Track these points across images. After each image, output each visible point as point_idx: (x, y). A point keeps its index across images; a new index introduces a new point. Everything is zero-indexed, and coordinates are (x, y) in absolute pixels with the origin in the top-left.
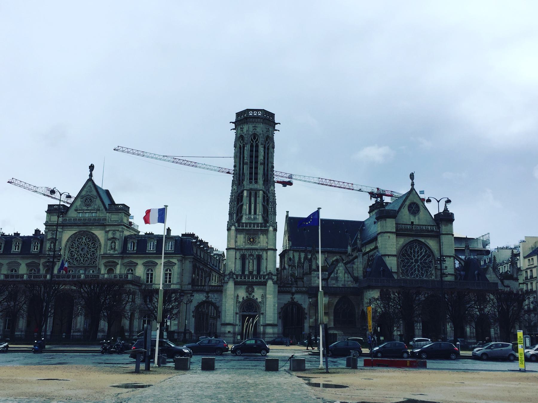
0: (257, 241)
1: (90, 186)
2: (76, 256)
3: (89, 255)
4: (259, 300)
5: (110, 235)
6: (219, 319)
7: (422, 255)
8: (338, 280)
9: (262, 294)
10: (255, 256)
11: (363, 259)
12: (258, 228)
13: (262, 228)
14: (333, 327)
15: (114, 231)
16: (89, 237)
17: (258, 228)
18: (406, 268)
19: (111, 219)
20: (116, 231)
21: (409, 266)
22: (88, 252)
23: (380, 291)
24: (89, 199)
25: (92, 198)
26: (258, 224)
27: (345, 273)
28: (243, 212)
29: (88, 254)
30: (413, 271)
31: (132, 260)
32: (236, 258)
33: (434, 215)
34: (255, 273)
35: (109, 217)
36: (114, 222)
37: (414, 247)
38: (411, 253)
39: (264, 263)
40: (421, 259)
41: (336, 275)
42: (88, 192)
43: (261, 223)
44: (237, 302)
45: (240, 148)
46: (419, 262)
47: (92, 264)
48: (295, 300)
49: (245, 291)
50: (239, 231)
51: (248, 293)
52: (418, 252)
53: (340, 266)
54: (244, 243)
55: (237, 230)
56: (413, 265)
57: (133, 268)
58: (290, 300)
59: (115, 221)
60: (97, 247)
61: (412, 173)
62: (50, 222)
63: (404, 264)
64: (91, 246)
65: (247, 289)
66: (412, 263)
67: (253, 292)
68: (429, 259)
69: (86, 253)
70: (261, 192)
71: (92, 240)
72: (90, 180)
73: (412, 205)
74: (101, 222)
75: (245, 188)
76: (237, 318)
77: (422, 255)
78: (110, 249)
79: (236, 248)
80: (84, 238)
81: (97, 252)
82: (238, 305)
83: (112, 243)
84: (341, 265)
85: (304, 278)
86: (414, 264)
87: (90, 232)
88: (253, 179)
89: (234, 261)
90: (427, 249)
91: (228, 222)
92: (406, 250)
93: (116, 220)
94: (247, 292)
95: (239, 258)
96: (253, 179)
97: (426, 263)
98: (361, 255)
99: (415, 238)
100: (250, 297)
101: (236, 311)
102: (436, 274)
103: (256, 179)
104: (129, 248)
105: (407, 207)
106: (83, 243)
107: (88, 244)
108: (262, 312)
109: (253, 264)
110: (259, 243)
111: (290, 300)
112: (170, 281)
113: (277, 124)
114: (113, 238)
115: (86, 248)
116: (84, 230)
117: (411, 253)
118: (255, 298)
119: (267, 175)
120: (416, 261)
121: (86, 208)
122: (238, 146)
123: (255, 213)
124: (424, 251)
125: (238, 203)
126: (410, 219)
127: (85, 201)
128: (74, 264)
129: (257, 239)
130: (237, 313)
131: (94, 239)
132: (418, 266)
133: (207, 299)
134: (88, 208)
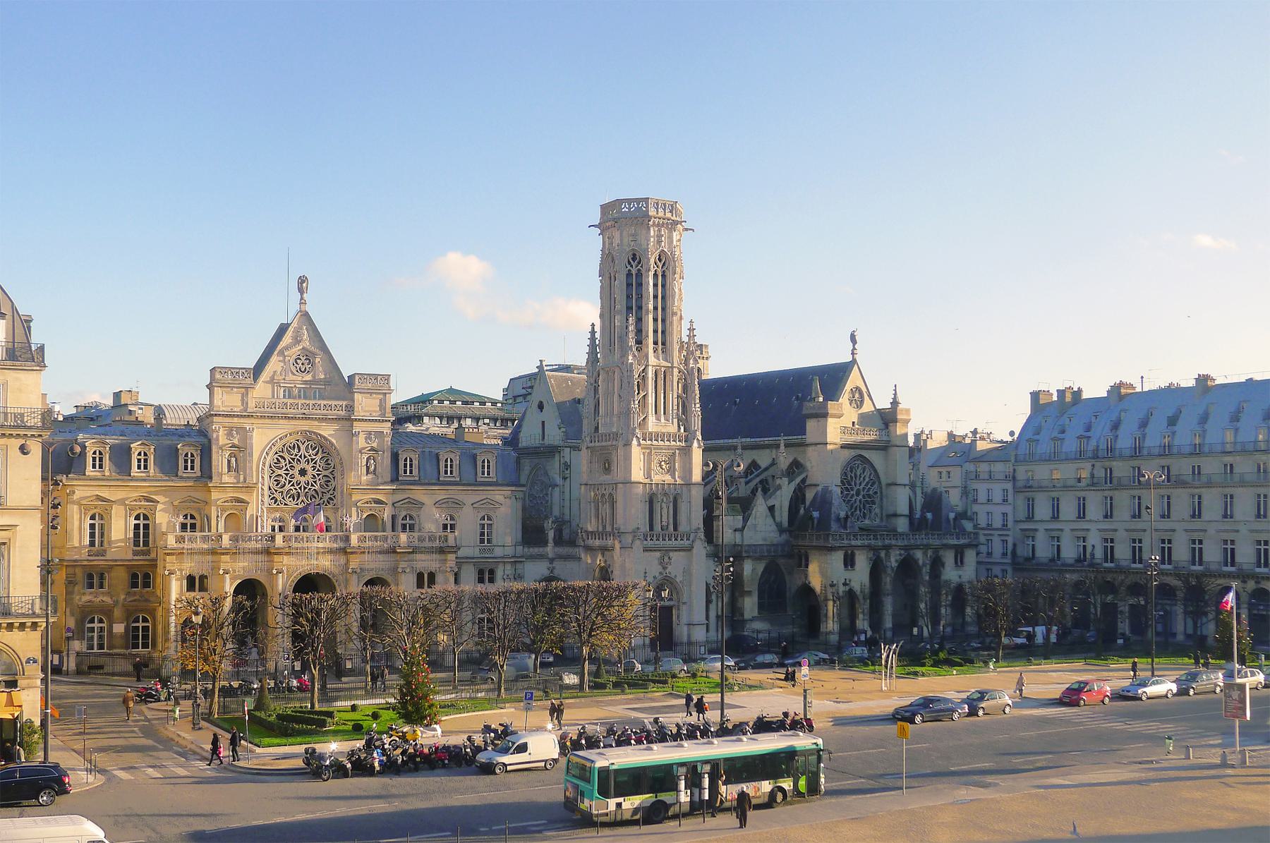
2: (287, 487)
10: (671, 496)
27: (766, 516)
34: (671, 527)
39: (683, 507)
45: (629, 275)
46: (862, 493)
47: (326, 505)
51: (662, 566)
52: (860, 477)
57: (414, 514)
62: (224, 409)
70: (676, 371)
80: (303, 448)
97: (869, 496)
102: (882, 514)
106: (300, 457)
107: (312, 460)
108: (685, 600)
112: (489, 541)
113: (687, 230)
118: (673, 576)
120: (858, 494)
121: (300, 378)
122: (625, 272)
128: (285, 504)
133: (552, 572)
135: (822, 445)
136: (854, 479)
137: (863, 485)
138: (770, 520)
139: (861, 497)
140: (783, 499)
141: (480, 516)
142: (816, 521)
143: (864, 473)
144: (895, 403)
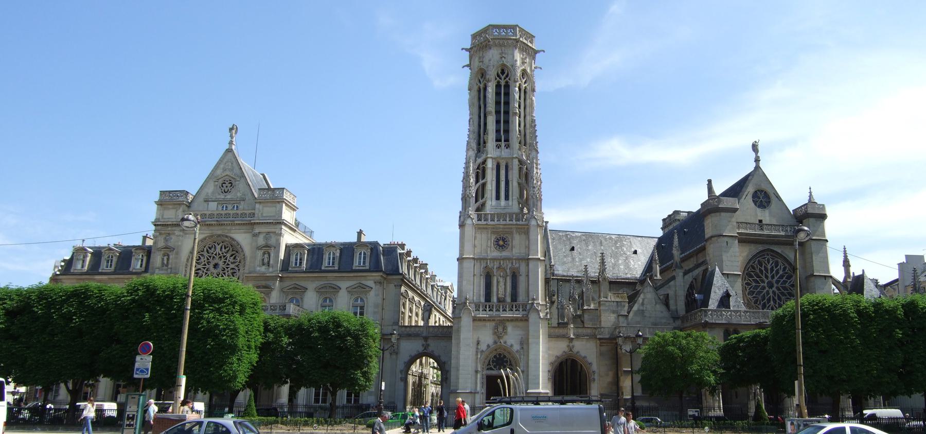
0: (511, 244)
1: (231, 159)
3: (226, 275)
4: (516, 347)
5: (261, 241)
6: (446, 383)
7: (779, 275)
8: (646, 316)
9: (522, 338)
10: (508, 271)
11: (684, 282)
12: (511, 222)
13: (518, 223)
14: (641, 396)
15: (267, 235)
16: (226, 246)
17: (511, 222)
18: (754, 295)
19: (262, 214)
20: (271, 234)
21: (760, 293)
22: (224, 270)
23: (723, 330)
24: (229, 182)
25: (233, 181)
26: (511, 215)
28: (485, 196)
29: (224, 273)
30: (766, 300)
31: (297, 283)
32: (474, 275)
33: (793, 211)
34: (508, 299)
35: (259, 211)
36: (268, 218)
37: (766, 262)
38: (761, 271)
40: (777, 282)
41: (641, 308)
42: (226, 170)
43: (517, 215)
44: (477, 352)
46: (775, 285)
48: (575, 350)
49: (491, 332)
50: (479, 228)
51: (497, 335)
52: (772, 270)
53: (647, 292)
54: (489, 249)
55: (478, 228)
56: (765, 291)
57: (298, 297)
58: (566, 349)
59: (270, 216)
60: (240, 262)
61: (755, 142)
63: (751, 289)
64: (229, 261)
65: (496, 328)
66: (764, 288)
67: (506, 333)
68: (790, 282)
69: (221, 272)
70: (516, 162)
71: (231, 249)
72: (229, 151)
73: (758, 193)
74: (246, 219)
75: (489, 156)
76: (478, 380)
77: (779, 275)
78: (261, 264)
79: (476, 257)
80: (218, 247)
81: (239, 270)
82: (479, 356)
83: (264, 253)
84: (649, 291)
85: (585, 316)
86: (767, 288)
87: (227, 237)
88: (503, 140)
89: (472, 280)
90: (786, 265)
91: (460, 212)
92: (753, 268)
93: (271, 215)
94: (495, 333)
95: (481, 275)
96: (503, 140)
97: (785, 288)
98: (682, 274)
99: (767, 247)
100: (500, 343)
101: (477, 367)
103: (507, 140)
104: (292, 262)
105: (751, 196)
107: (224, 256)
109: (505, 285)
110: (514, 247)
111: (566, 349)
114: (267, 246)
115: (221, 263)
116: (219, 232)
117: (761, 271)
119: (525, 135)
121: (223, 197)
123: (507, 198)
124: (782, 267)
125: (477, 181)
126: (756, 215)
127: (222, 186)
129: (510, 240)
130: (477, 372)
131: (234, 249)
132: (774, 292)
134: (225, 196)
135: (716, 238)
136: (764, 271)
137: (776, 278)
138: (660, 308)
139: (774, 289)
140: (677, 288)
141: (353, 297)
142: (699, 302)
143: (776, 267)
144: (811, 201)
